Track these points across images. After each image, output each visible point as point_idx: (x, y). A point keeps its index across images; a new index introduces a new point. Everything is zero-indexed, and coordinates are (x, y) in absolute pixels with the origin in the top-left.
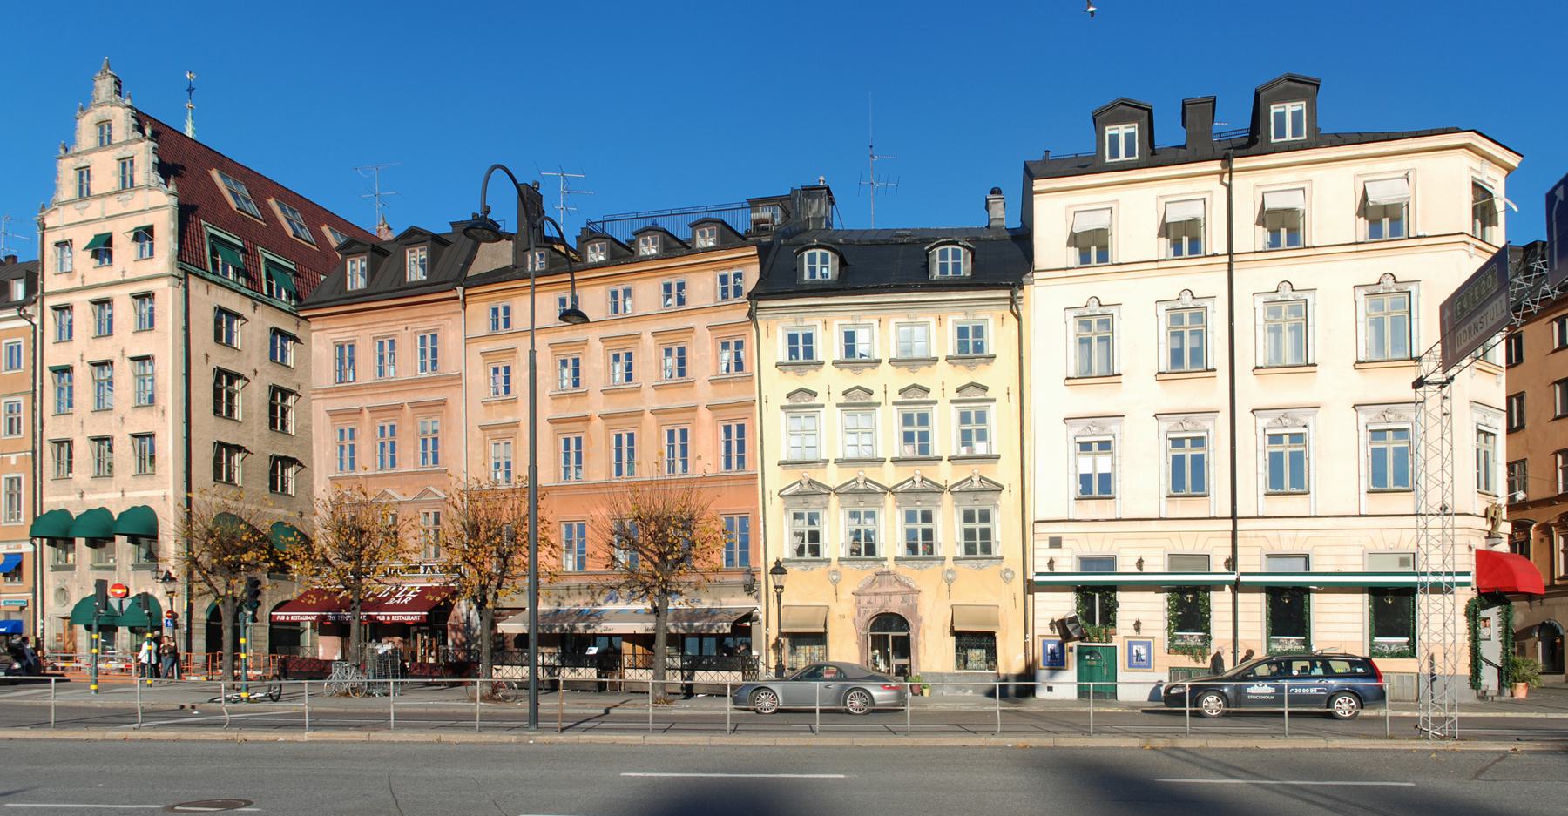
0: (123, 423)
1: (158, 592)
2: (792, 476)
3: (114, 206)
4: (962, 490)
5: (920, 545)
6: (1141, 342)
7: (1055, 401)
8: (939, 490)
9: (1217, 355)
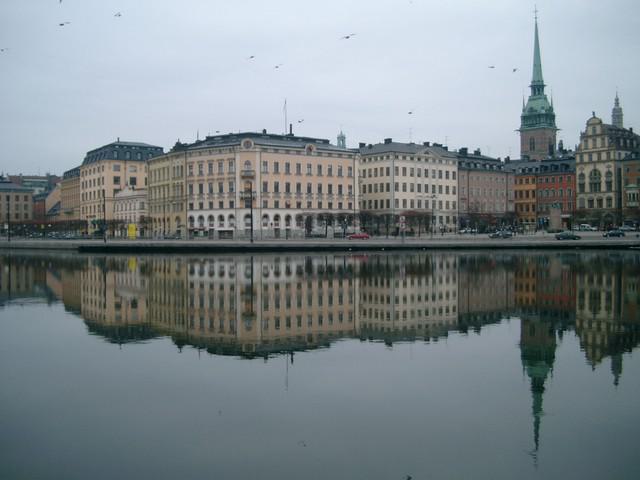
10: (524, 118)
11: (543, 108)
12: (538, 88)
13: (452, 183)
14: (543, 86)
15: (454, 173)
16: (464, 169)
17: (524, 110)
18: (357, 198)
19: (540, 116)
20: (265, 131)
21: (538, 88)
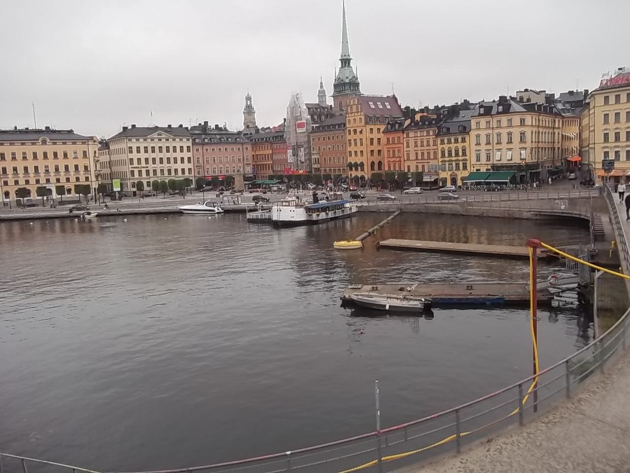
0: (359, 148)
1: (364, 175)
2: (442, 159)
3: (356, 114)
4: (463, 160)
5: (458, 168)
6: (483, 140)
7: (474, 147)
8: (460, 160)
9: (491, 142)
10: (335, 86)
11: (347, 78)
12: (346, 62)
13: (186, 155)
14: (349, 60)
15: (188, 147)
16: (198, 144)
17: (335, 80)
18: (93, 172)
19: (345, 84)
20: (16, 128)
21: (346, 62)
